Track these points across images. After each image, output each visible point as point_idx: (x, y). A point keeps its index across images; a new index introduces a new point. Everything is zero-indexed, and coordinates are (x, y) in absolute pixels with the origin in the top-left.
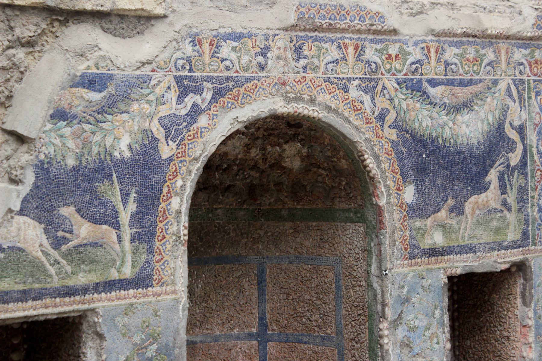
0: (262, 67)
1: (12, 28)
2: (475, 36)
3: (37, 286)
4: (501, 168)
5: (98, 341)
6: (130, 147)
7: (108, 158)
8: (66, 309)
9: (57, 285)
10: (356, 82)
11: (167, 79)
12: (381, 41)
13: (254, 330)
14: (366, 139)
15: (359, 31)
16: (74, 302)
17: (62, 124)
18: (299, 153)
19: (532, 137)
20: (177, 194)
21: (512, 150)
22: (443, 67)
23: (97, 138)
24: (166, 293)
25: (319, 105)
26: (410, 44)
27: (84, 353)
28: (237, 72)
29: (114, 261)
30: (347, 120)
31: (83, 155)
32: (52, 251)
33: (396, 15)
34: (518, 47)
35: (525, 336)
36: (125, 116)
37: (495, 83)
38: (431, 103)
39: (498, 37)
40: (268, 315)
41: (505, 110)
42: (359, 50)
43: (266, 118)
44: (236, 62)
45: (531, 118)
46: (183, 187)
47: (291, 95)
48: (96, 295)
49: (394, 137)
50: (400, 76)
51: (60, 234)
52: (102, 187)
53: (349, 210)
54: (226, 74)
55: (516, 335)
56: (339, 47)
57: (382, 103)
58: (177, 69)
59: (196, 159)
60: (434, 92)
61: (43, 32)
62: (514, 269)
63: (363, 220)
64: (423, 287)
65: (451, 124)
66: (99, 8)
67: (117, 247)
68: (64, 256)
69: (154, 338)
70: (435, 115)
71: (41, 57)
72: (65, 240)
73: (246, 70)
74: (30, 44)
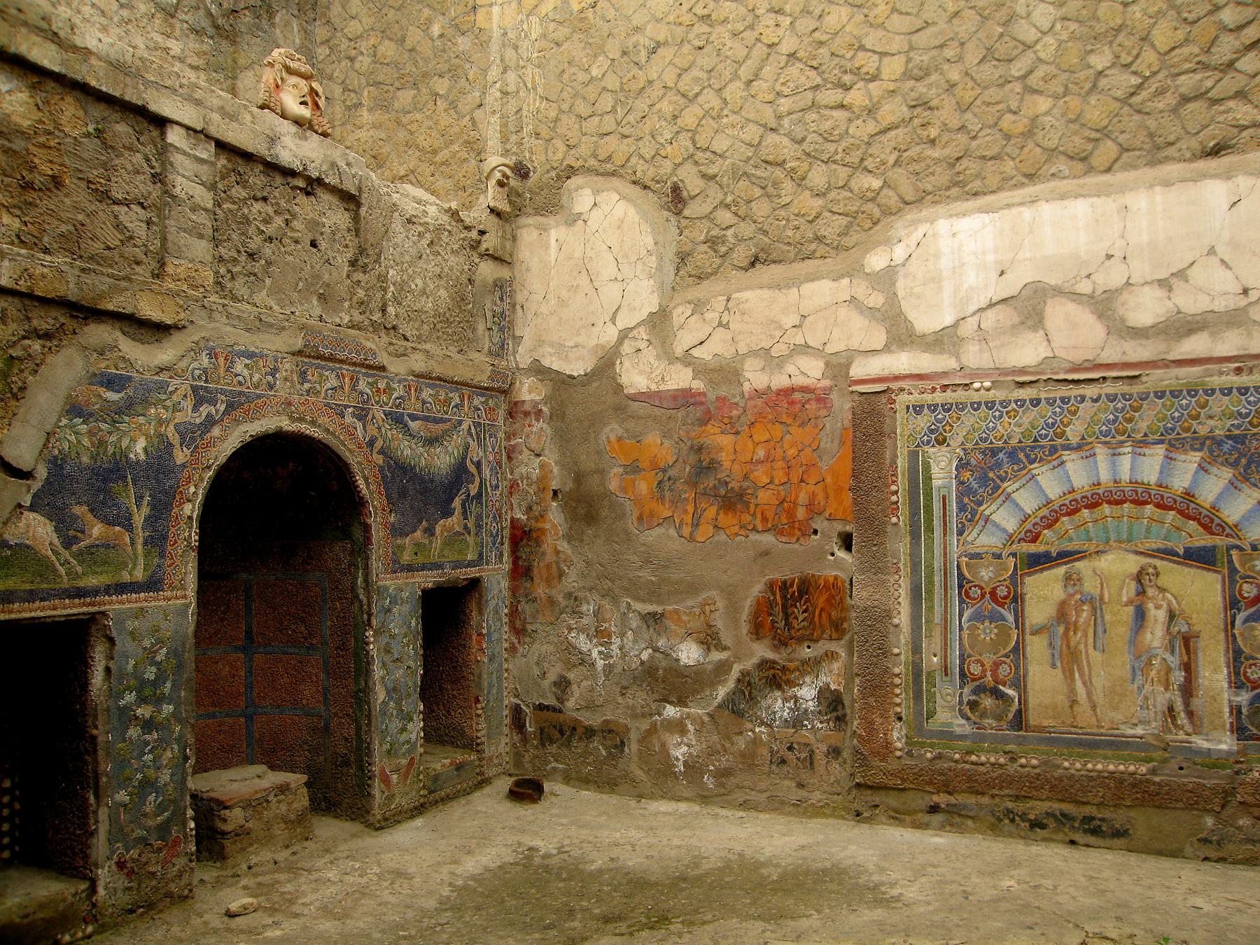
0: (271, 387)
1: (28, 319)
2: (445, 381)
4: (463, 497)
5: (107, 645)
6: (145, 449)
8: (75, 611)
10: (351, 410)
12: (373, 376)
14: (359, 463)
15: (355, 364)
16: (84, 605)
17: (78, 420)
19: (487, 472)
20: (189, 501)
22: (420, 405)
23: (113, 438)
24: (177, 598)
27: (91, 657)
28: (248, 388)
31: (98, 454)
32: (62, 550)
36: (141, 420)
37: (460, 423)
38: (410, 435)
39: (463, 384)
41: (467, 448)
42: (354, 381)
49: (381, 462)
50: (386, 408)
51: (71, 533)
52: (116, 487)
54: (239, 389)
57: (371, 430)
59: (209, 467)
60: (414, 425)
64: (402, 599)
69: (161, 642)
72: (76, 540)
74: (47, 336)
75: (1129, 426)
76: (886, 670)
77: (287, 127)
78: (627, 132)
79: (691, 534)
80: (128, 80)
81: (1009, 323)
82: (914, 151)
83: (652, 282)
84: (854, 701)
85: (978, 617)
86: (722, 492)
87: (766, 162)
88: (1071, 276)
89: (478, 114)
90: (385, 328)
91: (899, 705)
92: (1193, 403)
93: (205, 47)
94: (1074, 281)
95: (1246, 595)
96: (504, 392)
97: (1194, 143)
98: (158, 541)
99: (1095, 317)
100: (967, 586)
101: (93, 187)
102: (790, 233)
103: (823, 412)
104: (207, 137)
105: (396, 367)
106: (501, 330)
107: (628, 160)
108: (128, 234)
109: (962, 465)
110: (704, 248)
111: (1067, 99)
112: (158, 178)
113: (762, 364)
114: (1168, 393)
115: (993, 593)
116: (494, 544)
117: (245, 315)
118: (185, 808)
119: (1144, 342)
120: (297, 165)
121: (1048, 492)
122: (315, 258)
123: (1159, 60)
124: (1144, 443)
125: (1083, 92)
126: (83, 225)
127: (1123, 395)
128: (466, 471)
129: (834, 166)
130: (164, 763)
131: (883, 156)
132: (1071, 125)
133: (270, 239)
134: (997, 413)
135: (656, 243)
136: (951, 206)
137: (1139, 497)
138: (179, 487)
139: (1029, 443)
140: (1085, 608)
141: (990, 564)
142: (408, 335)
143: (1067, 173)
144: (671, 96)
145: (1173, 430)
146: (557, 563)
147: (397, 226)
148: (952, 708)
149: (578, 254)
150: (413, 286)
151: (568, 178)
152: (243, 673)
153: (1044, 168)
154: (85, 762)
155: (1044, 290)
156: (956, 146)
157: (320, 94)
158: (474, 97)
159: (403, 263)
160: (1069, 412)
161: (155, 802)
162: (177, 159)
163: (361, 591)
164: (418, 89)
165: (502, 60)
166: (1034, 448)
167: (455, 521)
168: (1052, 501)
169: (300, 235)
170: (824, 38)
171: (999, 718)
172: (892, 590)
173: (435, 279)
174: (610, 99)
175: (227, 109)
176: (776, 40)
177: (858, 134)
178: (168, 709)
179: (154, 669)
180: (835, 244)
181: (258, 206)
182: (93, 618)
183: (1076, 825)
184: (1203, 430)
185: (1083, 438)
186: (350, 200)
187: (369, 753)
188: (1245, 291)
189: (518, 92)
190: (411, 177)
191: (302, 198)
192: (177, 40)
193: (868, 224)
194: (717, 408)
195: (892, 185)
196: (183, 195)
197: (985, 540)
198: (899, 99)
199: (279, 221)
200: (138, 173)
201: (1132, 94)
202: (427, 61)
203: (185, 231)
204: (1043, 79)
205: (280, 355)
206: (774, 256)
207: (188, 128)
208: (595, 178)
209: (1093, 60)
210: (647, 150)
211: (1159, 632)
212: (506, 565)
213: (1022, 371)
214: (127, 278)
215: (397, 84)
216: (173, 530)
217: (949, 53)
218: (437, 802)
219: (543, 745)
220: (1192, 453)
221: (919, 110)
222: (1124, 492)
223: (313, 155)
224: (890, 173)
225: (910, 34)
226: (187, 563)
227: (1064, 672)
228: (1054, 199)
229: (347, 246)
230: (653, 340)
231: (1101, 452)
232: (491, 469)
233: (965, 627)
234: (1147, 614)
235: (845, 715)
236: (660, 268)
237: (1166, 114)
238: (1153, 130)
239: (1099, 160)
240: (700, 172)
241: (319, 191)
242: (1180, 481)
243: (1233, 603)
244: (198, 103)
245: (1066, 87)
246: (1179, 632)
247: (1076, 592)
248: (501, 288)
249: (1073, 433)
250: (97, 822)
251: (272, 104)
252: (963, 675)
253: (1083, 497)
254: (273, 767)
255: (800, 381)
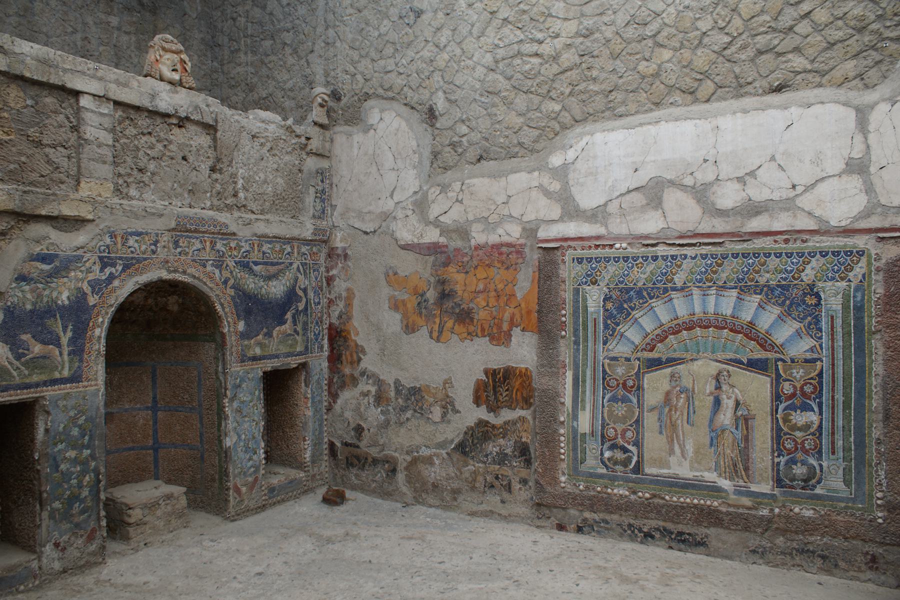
0: (154, 252)
3: (4, 383)
4: (293, 311)
6: (68, 298)
7: (54, 305)
8: (24, 397)
9: (18, 382)
10: (211, 262)
11: (94, 257)
12: (227, 239)
13: (150, 405)
14: (216, 295)
15: (213, 233)
16: (30, 393)
18: (177, 301)
19: (311, 294)
20: (99, 326)
21: (300, 301)
23: (47, 292)
24: (91, 386)
25: (189, 275)
26: (243, 241)
29: (57, 367)
30: (205, 284)
32: (15, 362)
33: (235, 225)
34: (304, 245)
35: (306, 403)
36: (66, 280)
37: (291, 264)
38: (254, 275)
39: (293, 239)
40: (158, 396)
41: (296, 279)
42: (213, 244)
43: (156, 282)
44: (138, 248)
45: (310, 284)
46: (103, 322)
47: (172, 269)
48: (45, 388)
49: (233, 294)
50: (237, 259)
51: (21, 351)
52: (49, 322)
53: (206, 335)
54: (131, 255)
55: (301, 403)
56: (201, 242)
57: (226, 274)
58: (100, 252)
59: (112, 306)
60: (255, 268)
61: (12, 227)
62: (300, 367)
63: (214, 341)
65: (266, 287)
66: (50, 214)
67: (59, 359)
68: (23, 364)
69: (82, 412)
70: (257, 281)
71: (10, 242)
72: (25, 355)
73: (144, 253)
75: (714, 276)
76: (556, 431)
77: (163, 86)
78: (401, 71)
79: (438, 337)
80: (52, 70)
81: (640, 204)
82: (581, 87)
83: (415, 172)
84: (536, 450)
85: (614, 399)
86: (457, 311)
87: (488, 92)
88: (680, 174)
89: (311, 57)
90: (237, 207)
91: (564, 454)
92: (757, 262)
93: (134, 19)
94: (681, 178)
95: (786, 392)
96: (325, 242)
97: (765, 83)
98: (78, 350)
99: (695, 201)
100: (608, 379)
101: (31, 139)
102: (502, 140)
103: (520, 260)
104: (108, 99)
105: (244, 233)
106: (323, 201)
107: (402, 89)
108: (55, 166)
109: (606, 299)
110: (448, 149)
111: (682, 51)
112: (75, 129)
113: (483, 227)
114: (740, 255)
115: (624, 384)
116: (317, 340)
117: (135, 209)
118: (99, 511)
119: (727, 219)
120: (171, 111)
121: (661, 318)
122: (184, 167)
123: (743, 25)
124: (723, 287)
125: (692, 47)
126: (24, 163)
127: (712, 255)
128: (296, 294)
129: (531, 96)
130: (85, 484)
131: (562, 89)
132: (684, 70)
133: (153, 158)
134: (630, 265)
135: (418, 146)
136: (605, 124)
137: (719, 323)
138: (91, 319)
139: (650, 285)
140: (682, 396)
141: (623, 365)
142: (254, 210)
143: (680, 102)
144: (430, 46)
145: (743, 279)
146: (357, 353)
147: (245, 141)
148: (596, 458)
149: (371, 152)
150: (257, 178)
151: (366, 100)
152: (151, 423)
153: (666, 98)
154: (34, 485)
155: (663, 182)
156: (609, 83)
157: (187, 62)
158: (308, 46)
159: (249, 164)
160: (676, 265)
161: (79, 507)
162: (87, 116)
163: (220, 374)
164: (274, 40)
165: (325, 22)
166: (653, 288)
167: (287, 327)
168: (663, 325)
169: (174, 154)
170: (526, 8)
171: (626, 466)
172: (561, 379)
173: (273, 172)
174: (391, 48)
175: (121, 80)
176: (495, 9)
177: (546, 74)
178: (87, 452)
179: (77, 429)
180: (531, 148)
181: (144, 138)
182: (36, 401)
183: (673, 537)
184: (762, 281)
185: (685, 283)
186: (210, 128)
187: (227, 476)
188: (794, 187)
189: (334, 43)
190: (270, 98)
191: (176, 130)
192: (115, 15)
193: (551, 135)
194: (454, 256)
195: (567, 108)
196: (91, 138)
197: (621, 349)
198: (574, 50)
199: (159, 146)
200: (61, 127)
201: (725, 49)
202: (279, 21)
203: (93, 160)
204: (666, 37)
205: (160, 232)
206: (492, 155)
207: (94, 95)
208: (382, 101)
209: (699, 24)
210: (414, 80)
211: (729, 413)
212: (326, 354)
213: (647, 237)
214: (54, 194)
215: (262, 37)
216: (88, 345)
217: (606, 19)
218: (275, 504)
219: (348, 468)
220: (755, 296)
221: (584, 59)
222: (709, 320)
223: (182, 103)
224: (566, 101)
225: (581, 5)
226: (98, 364)
227: (667, 437)
228: (670, 121)
229: (208, 157)
230: (416, 210)
231: (696, 292)
232: (315, 292)
233: (606, 404)
234: (722, 402)
235: (531, 458)
236: (420, 162)
237: (747, 63)
238: (737, 74)
239: (701, 94)
240: (447, 98)
241: (188, 125)
242: (747, 316)
243: (777, 397)
244: (101, 79)
245: (682, 43)
246: (742, 415)
247: (677, 386)
248: (322, 174)
249: (679, 280)
250: (41, 520)
251: (153, 73)
252: (603, 436)
253: (683, 323)
254: (169, 482)
255: (506, 239)
